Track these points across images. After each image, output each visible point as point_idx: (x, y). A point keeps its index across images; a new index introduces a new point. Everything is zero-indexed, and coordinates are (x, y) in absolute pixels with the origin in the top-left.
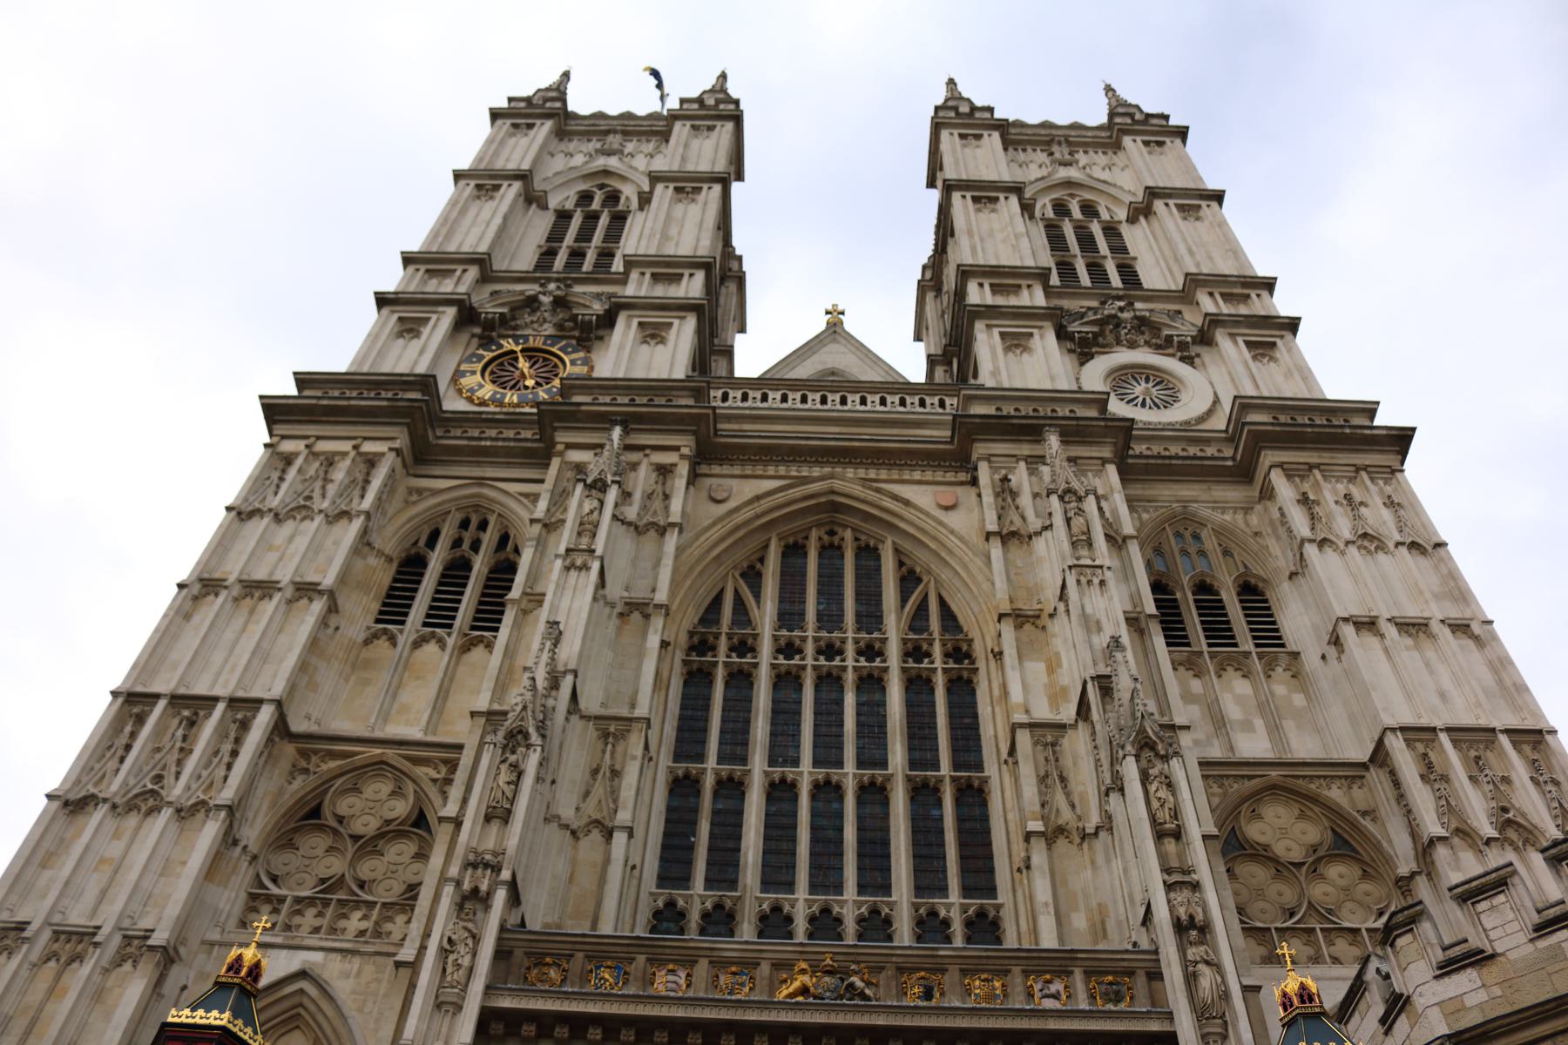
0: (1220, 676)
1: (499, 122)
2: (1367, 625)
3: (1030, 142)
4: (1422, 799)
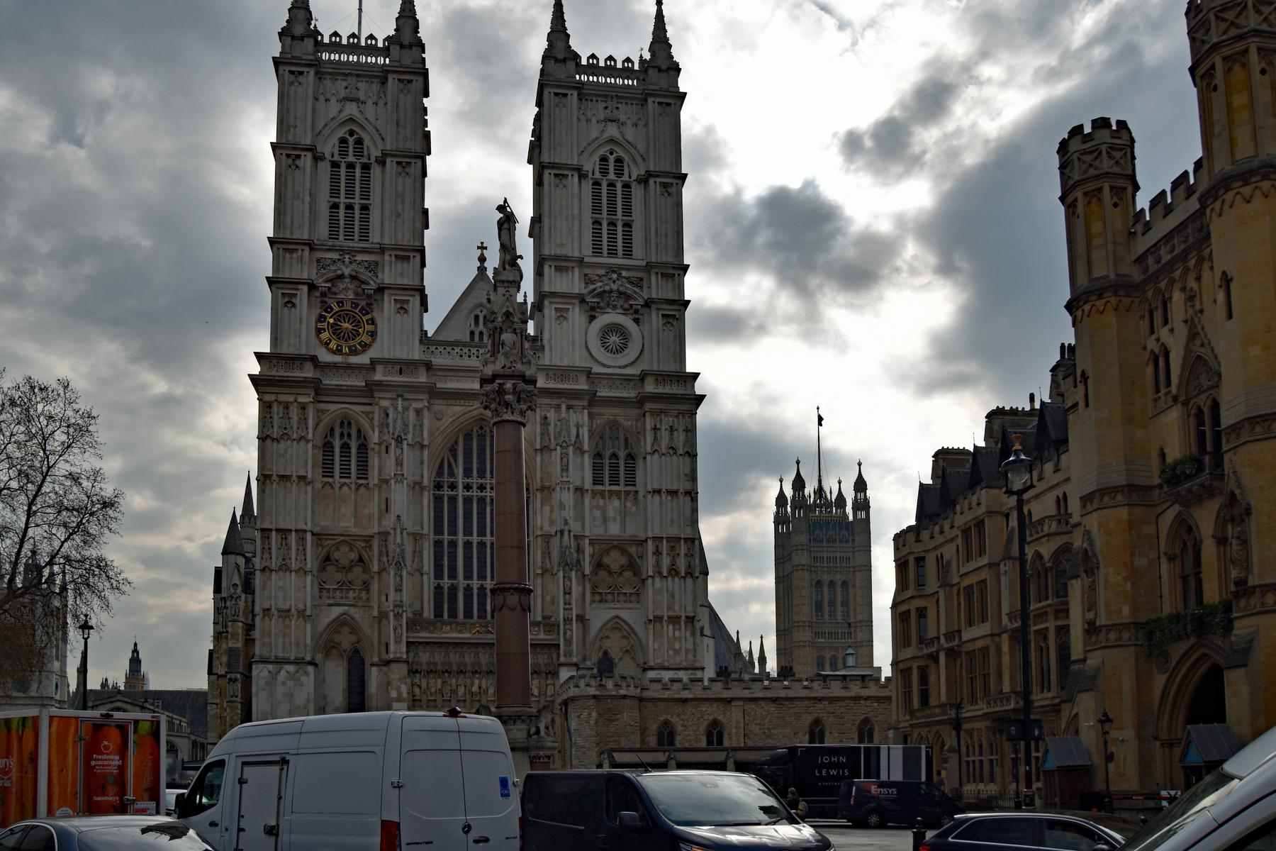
0: (610, 498)
1: (281, 68)
2: (659, 492)
3: (595, 95)
4: (651, 559)
